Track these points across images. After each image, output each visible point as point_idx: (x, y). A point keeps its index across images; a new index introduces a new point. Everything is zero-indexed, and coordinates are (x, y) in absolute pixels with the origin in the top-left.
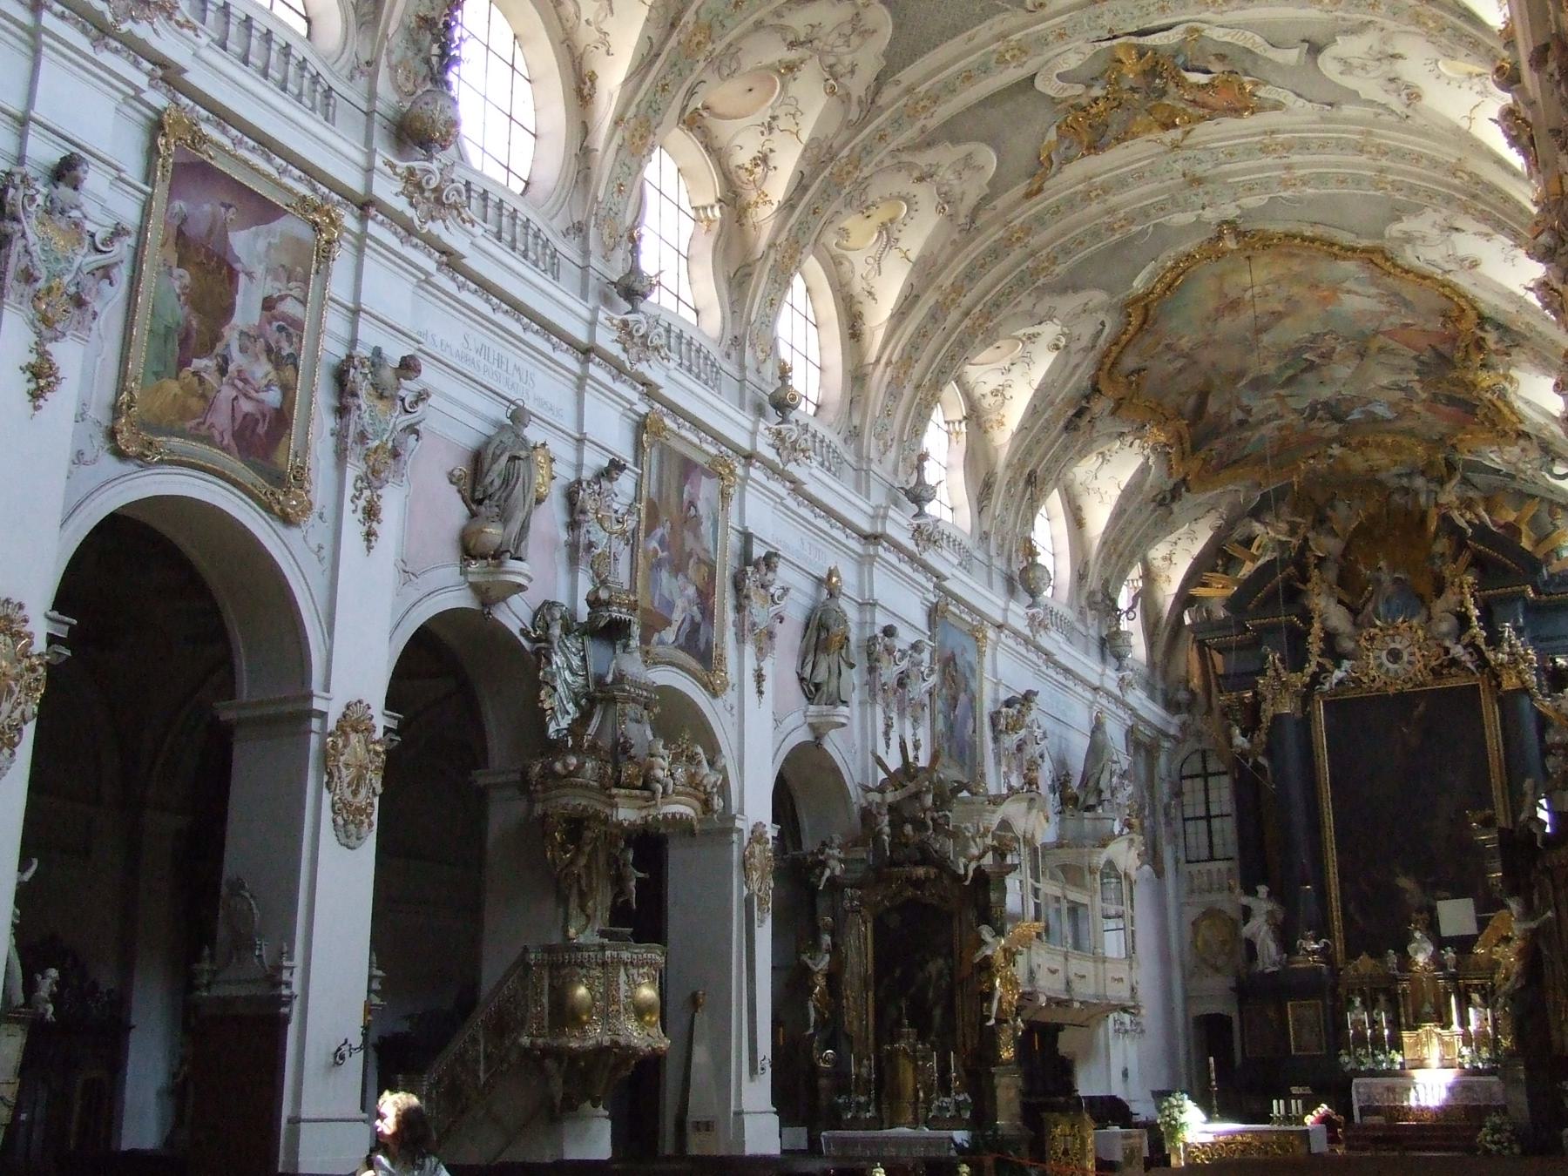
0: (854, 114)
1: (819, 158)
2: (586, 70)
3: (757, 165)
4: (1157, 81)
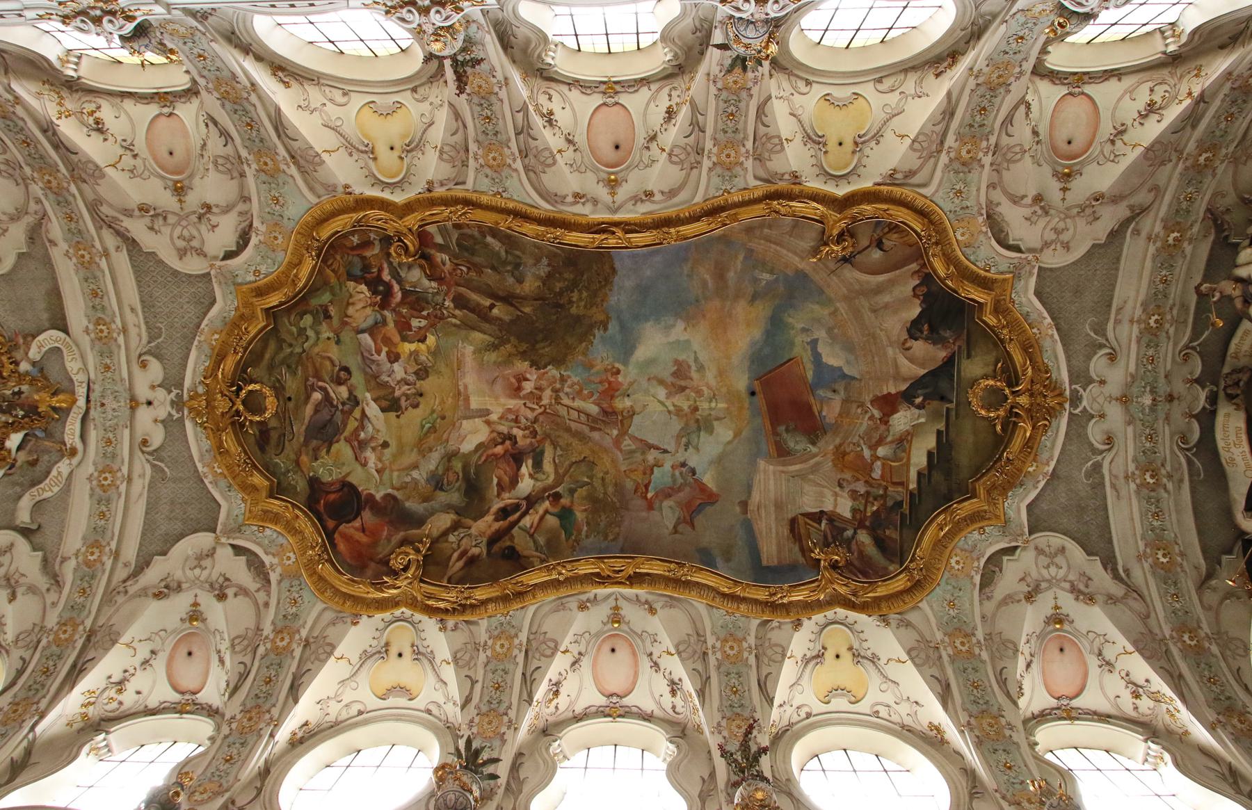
0: (105, 209)
1: (83, 171)
2: (293, 83)
3: (97, 123)
4: (22, 413)
